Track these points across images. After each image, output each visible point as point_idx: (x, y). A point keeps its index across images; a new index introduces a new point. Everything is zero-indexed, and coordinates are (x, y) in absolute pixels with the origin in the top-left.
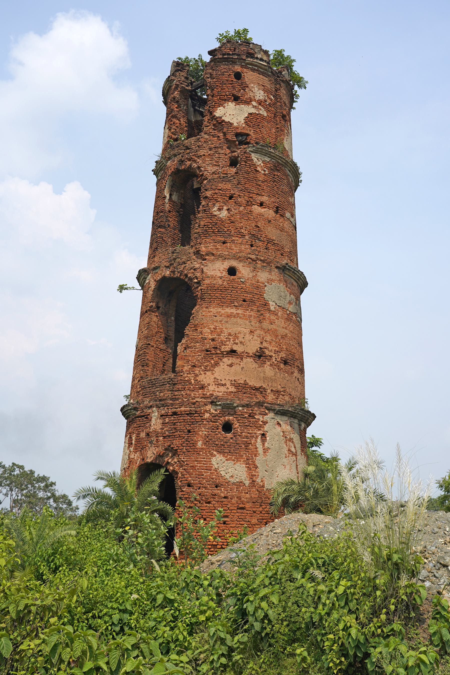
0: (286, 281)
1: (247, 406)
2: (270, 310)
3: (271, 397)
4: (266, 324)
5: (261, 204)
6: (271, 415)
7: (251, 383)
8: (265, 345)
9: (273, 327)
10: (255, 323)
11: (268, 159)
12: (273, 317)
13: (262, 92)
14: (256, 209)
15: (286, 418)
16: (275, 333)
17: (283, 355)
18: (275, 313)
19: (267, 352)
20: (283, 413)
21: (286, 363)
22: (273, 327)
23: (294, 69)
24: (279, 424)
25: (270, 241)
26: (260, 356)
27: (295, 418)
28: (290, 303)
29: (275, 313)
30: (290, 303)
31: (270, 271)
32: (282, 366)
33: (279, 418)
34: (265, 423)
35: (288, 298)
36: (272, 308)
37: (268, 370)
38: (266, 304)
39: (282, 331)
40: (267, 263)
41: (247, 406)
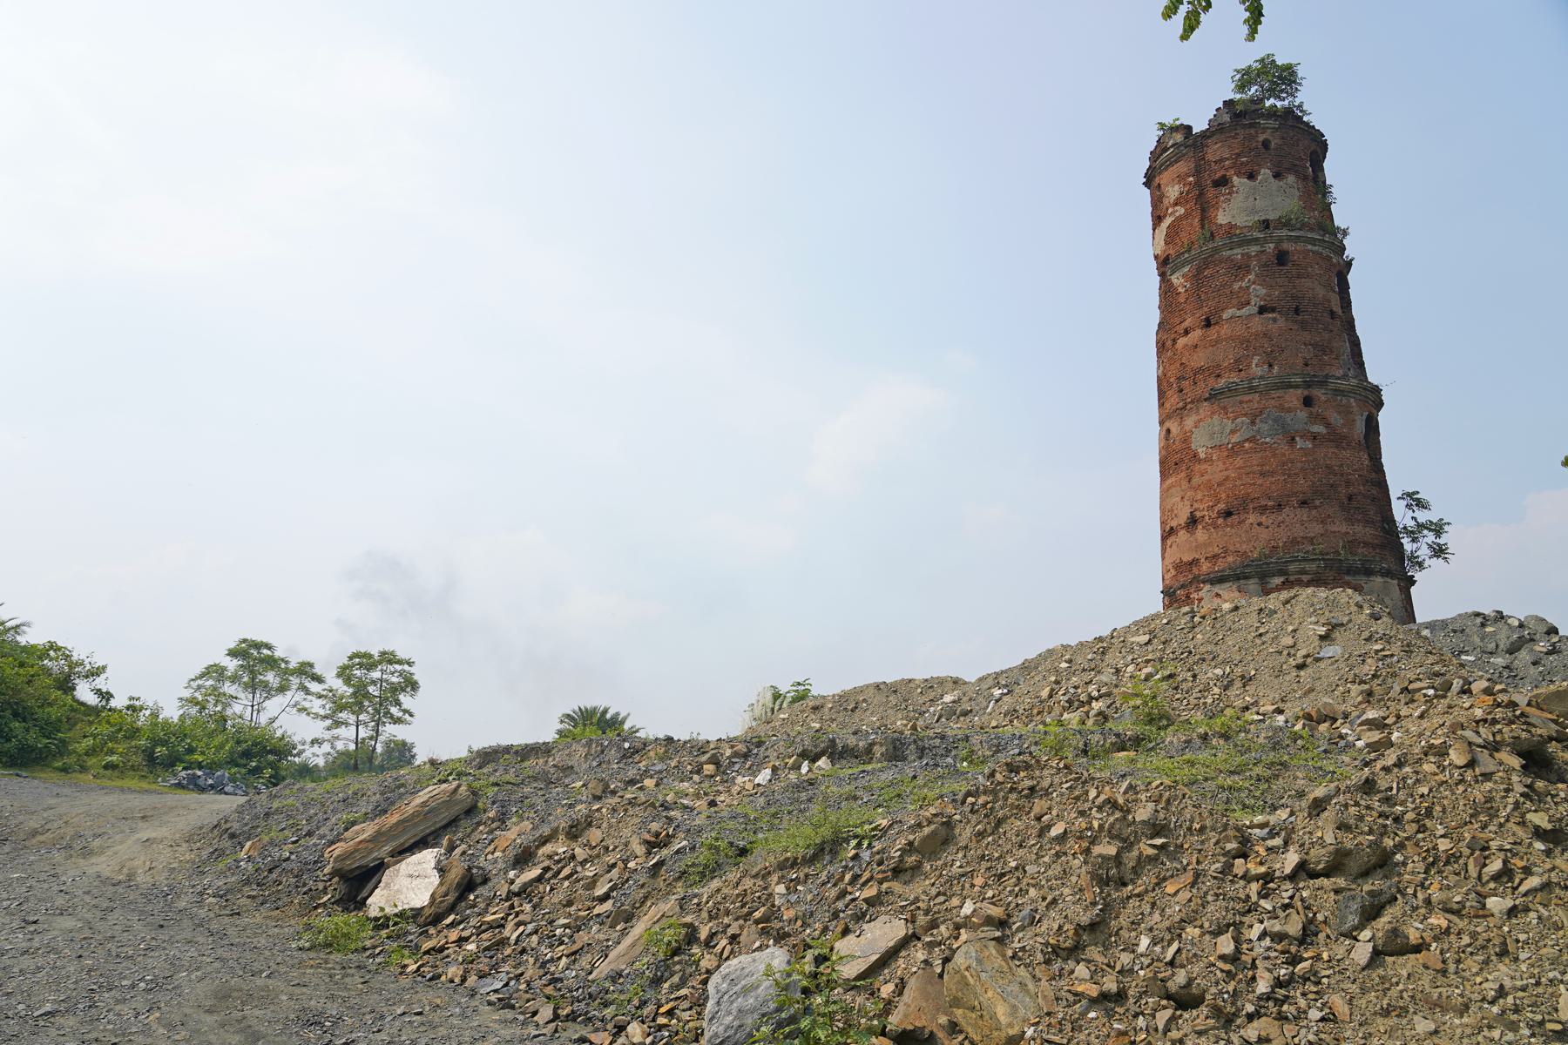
0: (1224, 408)
1: (1183, 587)
3: (1205, 567)
4: (1196, 480)
5: (1186, 332)
6: (1207, 587)
7: (1187, 558)
8: (1196, 505)
9: (1206, 477)
10: (1185, 484)
11: (1186, 269)
12: (1204, 467)
13: (1177, 187)
14: (1182, 342)
15: (1228, 585)
17: (1222, 506)
18: (1208, 460)
19: (1198, 514)
20: (1220, 580)
21: (1228, 514)
22: (1206, 477)
23: (1279, 63)
24: (1218, 595)
25: (1198, 371)
26: (1193, 522)
27: (1246, 578)
28: (1233, 432)
29: (1205, 460)
30: (1233, 432)
31: (1197, 412)
32: (1220, 521)
33: (1217, 589)
34: (1200, 600)
35: (1230, 426)
36: (1202, 456)
37: (1201, 534)
39: (1219, 477)
40: (1197, 401)
41: (1183, 587)
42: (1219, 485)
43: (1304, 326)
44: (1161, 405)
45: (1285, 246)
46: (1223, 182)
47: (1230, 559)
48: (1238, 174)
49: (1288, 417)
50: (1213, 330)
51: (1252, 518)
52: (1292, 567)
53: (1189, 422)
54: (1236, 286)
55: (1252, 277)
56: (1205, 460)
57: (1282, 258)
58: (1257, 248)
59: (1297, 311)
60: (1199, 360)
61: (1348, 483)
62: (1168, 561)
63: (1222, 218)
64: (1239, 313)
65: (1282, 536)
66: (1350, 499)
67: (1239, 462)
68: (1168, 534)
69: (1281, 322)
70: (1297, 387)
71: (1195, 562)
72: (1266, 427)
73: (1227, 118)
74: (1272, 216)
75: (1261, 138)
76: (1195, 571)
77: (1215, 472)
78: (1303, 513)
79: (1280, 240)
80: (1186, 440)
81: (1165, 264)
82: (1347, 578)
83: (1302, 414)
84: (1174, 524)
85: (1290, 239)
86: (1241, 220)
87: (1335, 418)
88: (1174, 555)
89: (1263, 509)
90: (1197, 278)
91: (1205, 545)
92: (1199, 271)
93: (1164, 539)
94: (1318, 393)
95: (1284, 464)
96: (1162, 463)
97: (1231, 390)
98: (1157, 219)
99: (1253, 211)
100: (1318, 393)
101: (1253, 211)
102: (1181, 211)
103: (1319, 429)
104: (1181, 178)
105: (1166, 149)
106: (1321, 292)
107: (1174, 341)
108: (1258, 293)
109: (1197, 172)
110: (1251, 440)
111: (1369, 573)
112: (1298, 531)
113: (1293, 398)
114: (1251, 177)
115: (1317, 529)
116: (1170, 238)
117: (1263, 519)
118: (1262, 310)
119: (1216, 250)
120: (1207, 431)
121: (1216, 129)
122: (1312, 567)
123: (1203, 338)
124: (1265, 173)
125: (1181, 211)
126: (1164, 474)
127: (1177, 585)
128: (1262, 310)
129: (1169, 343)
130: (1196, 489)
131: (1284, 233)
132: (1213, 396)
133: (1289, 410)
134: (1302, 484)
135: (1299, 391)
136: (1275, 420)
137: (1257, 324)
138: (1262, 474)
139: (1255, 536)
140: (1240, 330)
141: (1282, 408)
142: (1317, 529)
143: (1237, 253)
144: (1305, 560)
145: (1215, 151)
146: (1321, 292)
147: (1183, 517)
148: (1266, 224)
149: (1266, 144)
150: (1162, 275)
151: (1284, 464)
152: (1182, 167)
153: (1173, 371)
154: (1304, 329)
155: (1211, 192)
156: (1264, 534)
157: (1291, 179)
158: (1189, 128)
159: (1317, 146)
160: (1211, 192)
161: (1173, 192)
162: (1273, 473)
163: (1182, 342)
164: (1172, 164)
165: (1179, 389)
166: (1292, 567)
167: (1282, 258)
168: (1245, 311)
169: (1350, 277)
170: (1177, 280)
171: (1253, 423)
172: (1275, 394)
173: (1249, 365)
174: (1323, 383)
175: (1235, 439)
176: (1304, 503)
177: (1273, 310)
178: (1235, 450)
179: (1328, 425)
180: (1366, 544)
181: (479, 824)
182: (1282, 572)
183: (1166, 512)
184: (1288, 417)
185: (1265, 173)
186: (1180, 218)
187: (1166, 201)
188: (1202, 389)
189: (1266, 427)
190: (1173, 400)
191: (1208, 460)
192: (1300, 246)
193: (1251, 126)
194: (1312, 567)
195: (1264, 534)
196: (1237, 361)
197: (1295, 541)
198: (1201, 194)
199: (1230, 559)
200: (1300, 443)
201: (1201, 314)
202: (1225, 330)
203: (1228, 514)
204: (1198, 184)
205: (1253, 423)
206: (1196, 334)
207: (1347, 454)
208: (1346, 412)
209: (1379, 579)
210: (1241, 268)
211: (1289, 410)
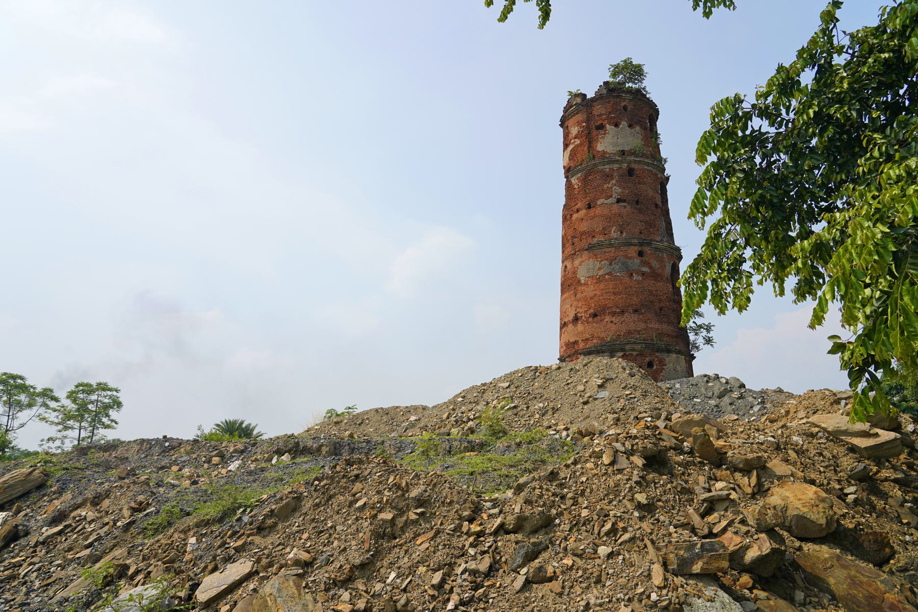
0: (596, 255)
2: (581, 284)
3: (582, 345)
4: (579, 296)
5: (578, 211)
7: (572, 340)
9: (584, 294)
10: (573, 298)
12: (583, 288)
14: (575, 216)
16: (585, 299)
17: (592, 311)
18: (586, 284)
19: (579, 315)
21: (595, 315)
22: (584, 294)
26: (576, 319)
27: (603, 352)
28: (600, 269)
29: (584, 284)
30: (600, 269)
32: (590, 319)
35: (598, 265)
36: (583, 282)
37: (580, 327)
38: (579, 281)
39: (592, 294)
40: (582, 250)
42: (591, 298)
43: (640, 211)
44: (563, 252)
45: (633, 166)
46: (601, 127)
47: (595, 341)
48: (610, 124)
49: (630, 262)
50: (592, 210)
51: (608, 318)
52: (628, 347)
53: (577, 262)
54: (605, 186)
55: (614, 182)
56: (584, 284)
57: (631, 172)
58: (618, 166)
59: (637, 202)
60: (584, 227)
61: (660, 301)
62: (563, 341)
63: (600, 147)
64: (606, 202)
65: (624, 329)
66: (661, 309)
67: (602, 286)
68: (563, 325)
69: (628, 208)
70: (635, 245)
71: (576, 342)
72: (617, 267)
73: (605, 91)
74: (626, 149)
75: (623, 104)
76: (576, 347)
77: (589, 291)
78: (635, 317)
79: (630, 162)
80: (575, 273)
81: (568, 171)
82: (657, 354)
83: (637, 261)
84: (566, 320)
85: (635, 162)
86: (610, 149)
87: (655, 264)
88: (565, 340)
89: (614, 314)
90: (585, 181)
91: (582, 333)
92: (586, 176)
93: (561, 328)
94: (647, 249)
95: (626, 288)
96: (562, 285)
97: (600, 245)
98: (566, 146)
99: (616, 145)
100: (647, 249)
101: (616, 145)
102: (578, 142)
103: (645, 269)
104: (579, 123)
105: (572, 106)
106: (651, 193)
107: (571, 215)
108: (617, 191)
109: (588, 120)
110: (609, 274)
111: (669, 351)
112: (632, 327)
113: (633, 251)
114: (616, 125)
115: (642, 326)
116: (572, 156)
117: (614, 319)
118: (619, 201)
119: (595, 165)
120: (586, 268)
121: (599, 97)
122: (638, 347)
123: (587, 214)
124: (624, 124)
125: (578, 142)
126: (563, 292)
127: (566, 355)
128: (619, 201)
129: (568, 216)
130: (579, 301)
131: (632, 158)
132: (590, 248)
133: (630, 258)
134: (635, 300)
135: (636, 248)
136: (623, 264)
137: (616, 208)
138: (614, 293)
139: (608, 328)
140: (606, 211)
141: (626, 257)
142: (642, 326)
143: (607, 168)
144: (634, 343)
145: (598, 109)
146: (651, 193)
147: (571, 317)
148: (623, 153)
149: (625, 108)
150: (567, 177)
151: (626, 288)
152: (579, 117)
153: (570, 232)
154: (640, 213)
155: (595, 132)
156: (614, 328)
157: (638, 128)
158: (585, 95)
159: (653, 113)
160: (595, 132)
161: (574, 131)
162: (620, 293)
163: (575, 216)
164: (574, 115)
165: (575, 243)
166: (628, 347)
167: (631, 172)
168: (610, 201)
169: (668, 187)
170: (574, 181)
171: (611, 264)
172: (623, 248)
173: (610, 232)
174: (649, 244)
175: (601, 273)
176: (636, 311)
177: (624, 201)
178: (599, 280)
179: (651, 268)
180: (668, 335)
181: (44, 495)
182: (622, 350)
183: (563, 313)
184: (630, 262)
185: (624, 124)
186: (577, 146)
187: (570, 136)
188: (584, 244)
189: (617, 267)
190: (569, 249)
191: (586, 284)
192: (641, 166)
193: (618, 97)
194: (638, 347)
195: (614, 328)
196: (604, 229)
197: (630, 332)
198: (589, 133)
199: (595, 341)
200: (635, 277)
201: (586, 201)
202: (598, 211)
203: (595, 315)
204: (588, 127)
205: (611, 264)
206: (583, 212)
207: (660, 284)
208: (661, 261)
209: (674, 355)
210: (608, 177)
211: (630, 258)
